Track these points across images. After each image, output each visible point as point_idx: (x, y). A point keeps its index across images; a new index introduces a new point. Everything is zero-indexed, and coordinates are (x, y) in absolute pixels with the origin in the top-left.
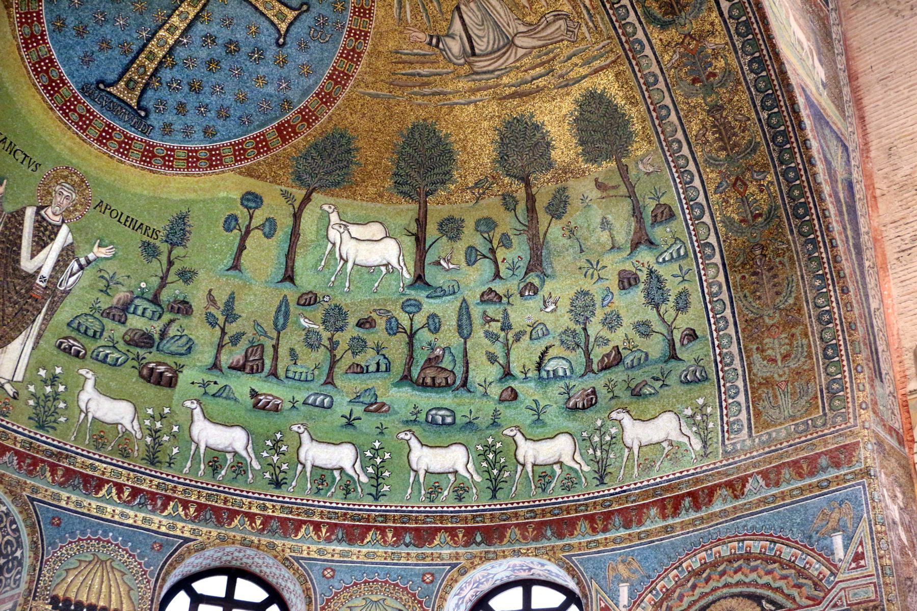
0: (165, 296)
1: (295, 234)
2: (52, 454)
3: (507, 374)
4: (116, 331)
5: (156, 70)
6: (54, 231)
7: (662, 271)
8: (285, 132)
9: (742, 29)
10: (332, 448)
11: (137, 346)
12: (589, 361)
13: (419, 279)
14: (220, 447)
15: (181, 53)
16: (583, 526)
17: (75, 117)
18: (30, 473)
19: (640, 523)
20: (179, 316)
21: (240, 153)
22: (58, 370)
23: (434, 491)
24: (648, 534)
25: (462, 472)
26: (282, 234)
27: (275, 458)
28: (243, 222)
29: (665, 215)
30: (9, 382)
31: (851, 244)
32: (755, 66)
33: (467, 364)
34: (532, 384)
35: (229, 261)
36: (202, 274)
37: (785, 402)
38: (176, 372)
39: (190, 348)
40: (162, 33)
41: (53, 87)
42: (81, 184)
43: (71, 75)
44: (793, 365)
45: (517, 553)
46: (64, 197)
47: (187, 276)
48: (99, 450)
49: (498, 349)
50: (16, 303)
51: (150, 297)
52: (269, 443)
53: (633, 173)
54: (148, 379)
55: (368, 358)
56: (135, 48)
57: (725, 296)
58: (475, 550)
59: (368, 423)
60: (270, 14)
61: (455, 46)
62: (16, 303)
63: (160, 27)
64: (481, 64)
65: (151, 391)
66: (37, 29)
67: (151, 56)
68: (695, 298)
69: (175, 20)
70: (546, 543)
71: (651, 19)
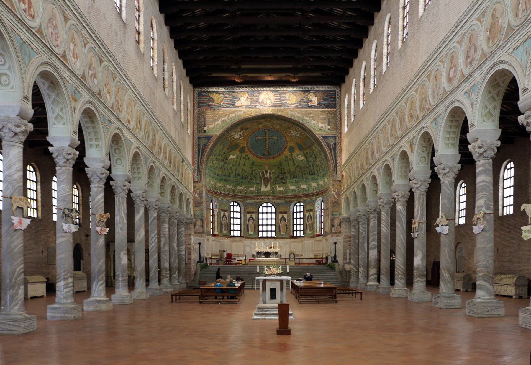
0: (282, 172)
1: (293, 159)
3: (318, 172)
4: (278, 179)
6: (267, 171)
8: (285, 148)
21: (282, 153)
26: (291, 160)
35: (287, 165)
38: (286, 181)
41: (259, 157)
46: (267, 167)
47: (284, 169)
55: (306, 172)
59: (307, 181)
65: (285, 185)
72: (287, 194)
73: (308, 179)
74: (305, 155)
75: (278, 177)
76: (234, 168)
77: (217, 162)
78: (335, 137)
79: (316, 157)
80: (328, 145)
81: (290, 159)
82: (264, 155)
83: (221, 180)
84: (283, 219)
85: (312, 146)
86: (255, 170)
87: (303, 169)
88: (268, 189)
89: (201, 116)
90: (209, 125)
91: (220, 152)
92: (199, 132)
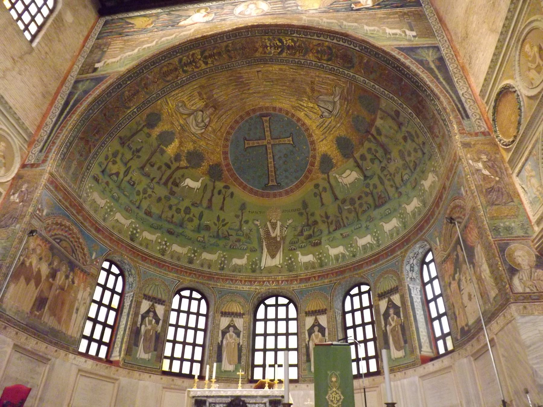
1: (331, 187)
2: (295, 277)
3: (397, 188)
4: (302, 238)
5: (275, 173)
7: (409, 129)
8: (313, 165)
9: (366, 50)
12: (410, 169)
13: (365, 177)
15: (277, 166)
16: (425, 224)
19: (434, 215)
21: (307, 177)
23: (392, 235)
24: (437, 217)
25: (397, 226)
29: (397, 113)
30: (280, 264)
31: (441, 79)
32: (377, 56)
33: (387, 192)
35: (320, 204)
37: (444, 147)
39: (321, 233)
41: (256, 193)
44: (441, 134)
45: (415, 243)
47: (313, 214)
49: (392, 183)
53: (383, 109)
56: (267, 172)
57: (422, 125)
58: (406, 247)
59: (371, 225)
60: (286, 142)
61: (326, 114)
64: (335, 112)
67: (271, 171)
68: (418, 131)
69: (269, 160)
70: (419, 236)
71: (349, 68)
72: (325, 268)
75: (301, 233)
76: (195, 211)
77: (145, 181)
78: (437, 48)
79: (387, 152)
80: (422, 63)
81: (325, 189)
82: (266, 187)
84: (316, 329)
85: (374, 121)
86: (247, 222)
88: (278, 260)
90: (108, 59)
91: (153, 154)
92: (82, 71)
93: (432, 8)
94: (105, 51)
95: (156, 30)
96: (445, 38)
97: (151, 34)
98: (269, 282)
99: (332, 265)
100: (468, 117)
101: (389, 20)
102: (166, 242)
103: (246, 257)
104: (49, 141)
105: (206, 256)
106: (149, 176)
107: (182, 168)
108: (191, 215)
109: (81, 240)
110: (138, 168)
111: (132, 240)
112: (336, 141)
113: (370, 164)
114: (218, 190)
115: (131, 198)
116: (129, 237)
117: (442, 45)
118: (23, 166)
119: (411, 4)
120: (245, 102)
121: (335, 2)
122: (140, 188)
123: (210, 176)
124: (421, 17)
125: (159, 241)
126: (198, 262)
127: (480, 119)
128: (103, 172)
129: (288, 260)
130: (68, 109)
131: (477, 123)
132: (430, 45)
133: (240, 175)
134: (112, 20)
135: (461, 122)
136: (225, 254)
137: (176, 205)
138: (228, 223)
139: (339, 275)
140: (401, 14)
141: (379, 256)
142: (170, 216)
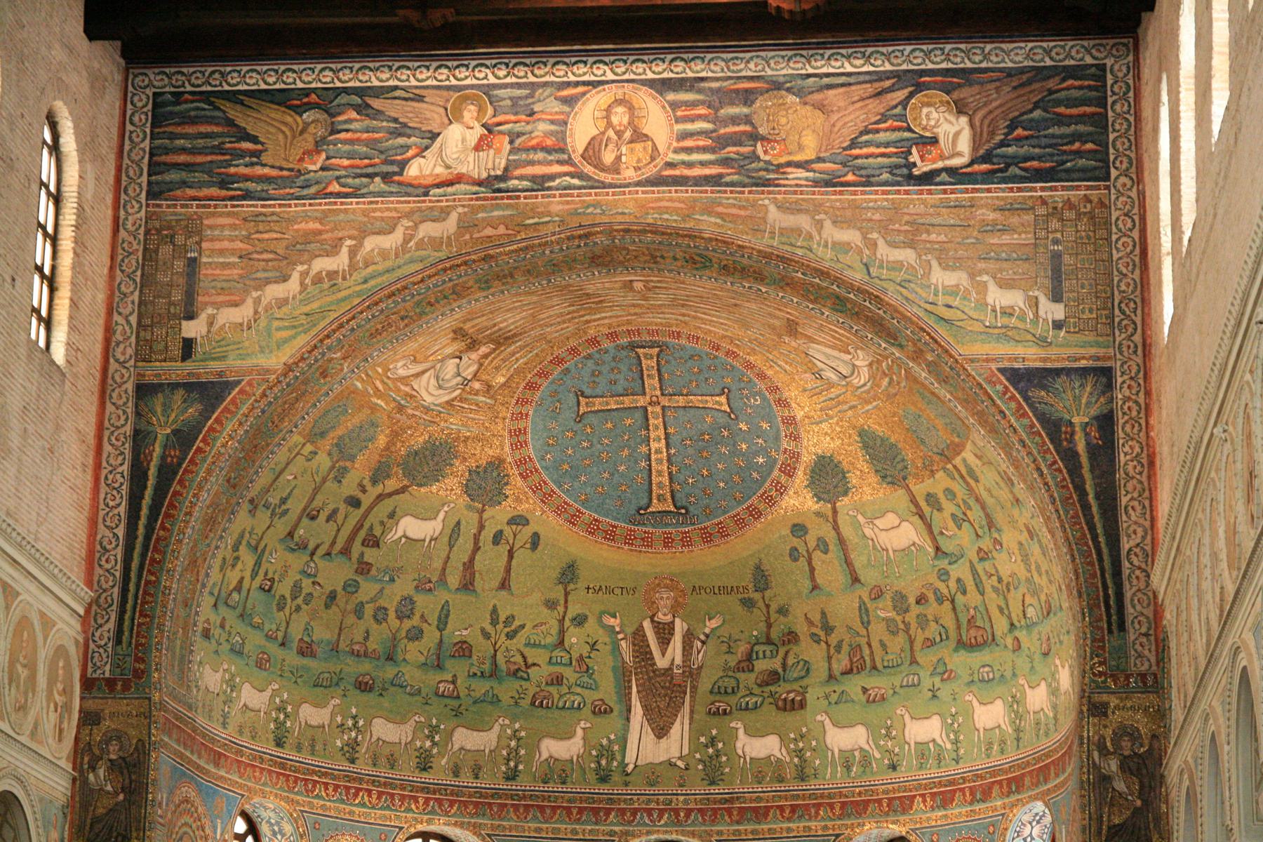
0: (775, 634)
1: (842, 541)
2: (726, 801)
3: (1012, 625)
4: (748, 679)
8: (789, 471)
10: (926, 722)
11: (767, 684)
13: (938, 549)
14: (849, 747)
17: (639, 542)
18: (713, 822)
20: (791, 646)
21: (771, 502)
22: (714, 732)
23: (990, 745)
25: (1003, 727)
27: (889, 744)
28: (802, 550)
30: (680, 758)
31: (1091, 497)
34: (1024, 632)
35: (808, 584)
36: (794, 603)
38: (803, 694)
40: (653, 457)
41: (610, 535)
42: (671, 583)
43: (618, 520)
47: (783, 611)
48: (760, 783)
50: (666, 695)
51: (763, 640)
52: (883, 731)
54: (785, 710)
55: (933, 630)
58: (1013, 798)
60: (710, 405)
62: (666, 695)
63: (650, 455)
65: (791, 718)
66: (571, 511)
67: (660, 473)
69: (654, 445)
72: (812, 784)
73: (947, 675)
74: (920, 513)
75: (747, 662)
76: (427, 605)
77: (297, 561)
79: (991, 524)
81: (823, 546)
83: (324, 685)
85: (958, 449)
86: (580, 621)
87: (915, 610)
89: (166, 251)
90: (218, 306)
91: (316, 491)
93: (1134, 194)
94: (194, 260)
95: (335, 187)
96: (1137, 338)
97: (323, 205)
98: (649, 812)
99: (831, 778)
100: (1122, 627)
101: (1006, 239)
102: (354, 717)
103: (580, 732)
104: (129, 606)
105: (465, 739)
106: (305, 548)
107: (390, 495)
108: (416, 621)
109: (200, 809)
110: (282, 541)
111: (279, 743)
112: (860, 435)
113: (951, 524)
114: (494, 531)
115: (267, 627)
116: (271, 736)
117: (1122, 366)
118: (88, 684)
119: (1082, 162)
120: (588, 322)
121: (866, 131)
122: (284, 589)
123: (469, 495)
124: (1098, 219)
125: (339, 719)
126: (443, 762)
127: (1146, 635)
128: (215, 605)
129: (707, 746)
130: (149, 493)
131: (1138, 647)
132: (1090, 363)
133: (560, 487)
134: (178, 96)
135: (1103, 640)
136: (517, 726)
137: (373, 600)
138: (523, 626)
139: (849, 816)
140: (1042, 211)
141: (955, 791)
142: (359, 637)
